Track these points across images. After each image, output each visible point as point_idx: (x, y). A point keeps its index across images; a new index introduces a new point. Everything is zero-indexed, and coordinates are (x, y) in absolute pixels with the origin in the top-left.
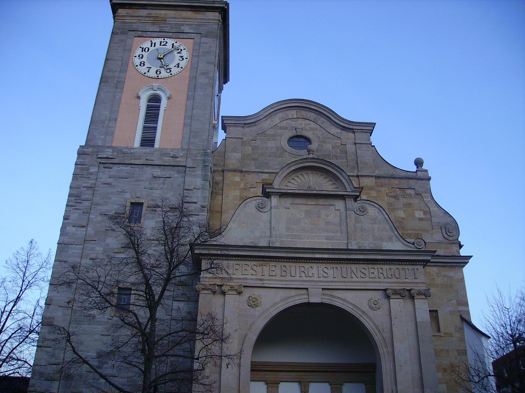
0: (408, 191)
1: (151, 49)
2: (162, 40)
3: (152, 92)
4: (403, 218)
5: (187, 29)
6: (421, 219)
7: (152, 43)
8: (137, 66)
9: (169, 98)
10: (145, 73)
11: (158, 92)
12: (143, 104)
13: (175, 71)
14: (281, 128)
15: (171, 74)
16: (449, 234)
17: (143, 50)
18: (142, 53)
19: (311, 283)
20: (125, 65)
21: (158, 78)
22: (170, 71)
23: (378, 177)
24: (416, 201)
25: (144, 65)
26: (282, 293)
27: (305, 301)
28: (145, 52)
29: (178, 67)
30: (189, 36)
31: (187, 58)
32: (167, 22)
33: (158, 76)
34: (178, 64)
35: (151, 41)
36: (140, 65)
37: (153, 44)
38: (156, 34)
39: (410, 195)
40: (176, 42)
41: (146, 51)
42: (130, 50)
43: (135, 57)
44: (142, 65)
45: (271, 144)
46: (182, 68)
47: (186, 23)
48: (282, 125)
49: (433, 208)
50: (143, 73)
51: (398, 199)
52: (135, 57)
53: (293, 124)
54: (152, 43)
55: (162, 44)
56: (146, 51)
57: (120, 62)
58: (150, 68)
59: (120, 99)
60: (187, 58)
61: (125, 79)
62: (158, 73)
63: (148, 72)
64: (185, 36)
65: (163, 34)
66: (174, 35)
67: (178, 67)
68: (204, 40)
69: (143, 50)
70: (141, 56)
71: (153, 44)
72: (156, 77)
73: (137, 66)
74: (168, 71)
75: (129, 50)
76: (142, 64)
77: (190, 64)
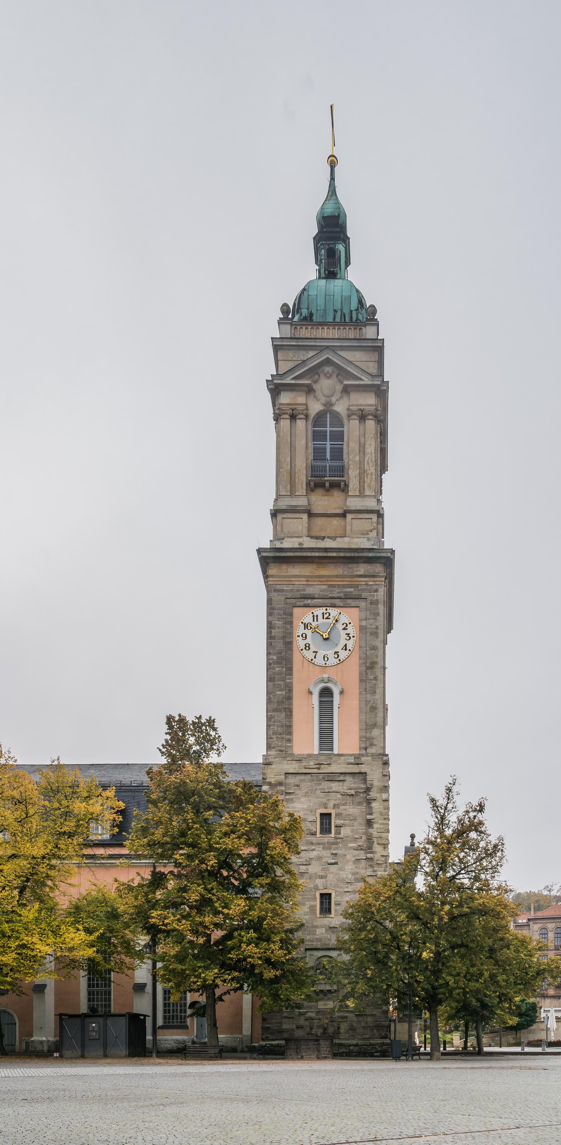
3: (323, 685)
7: (313, 616)
8: (302, 650)
9: (342, 693)
10: (312, 660)
11: (329, 685)
12: (315, 699)
13: (343, 655)
15: (340, 660)
17: (306, 626)
25: (309, 649)
29: (346, 649)
34: (346, 645)
35: (313, 613)
36: (305, 648)
41: (309, 628)
43: (298, 636)
44: (307, 648)
46: (350, 650)
50: (310, 660)
52: (298, 636)
55: (326, 616)
56: (309, 628)
58: (317, 652)
60: (353, 637)
63: (315, 657)
67: (346, 649)
70: (304, 635)
73: (302, 650)
74: (336, 656)
76: (307, 647)
77: (358, 640)
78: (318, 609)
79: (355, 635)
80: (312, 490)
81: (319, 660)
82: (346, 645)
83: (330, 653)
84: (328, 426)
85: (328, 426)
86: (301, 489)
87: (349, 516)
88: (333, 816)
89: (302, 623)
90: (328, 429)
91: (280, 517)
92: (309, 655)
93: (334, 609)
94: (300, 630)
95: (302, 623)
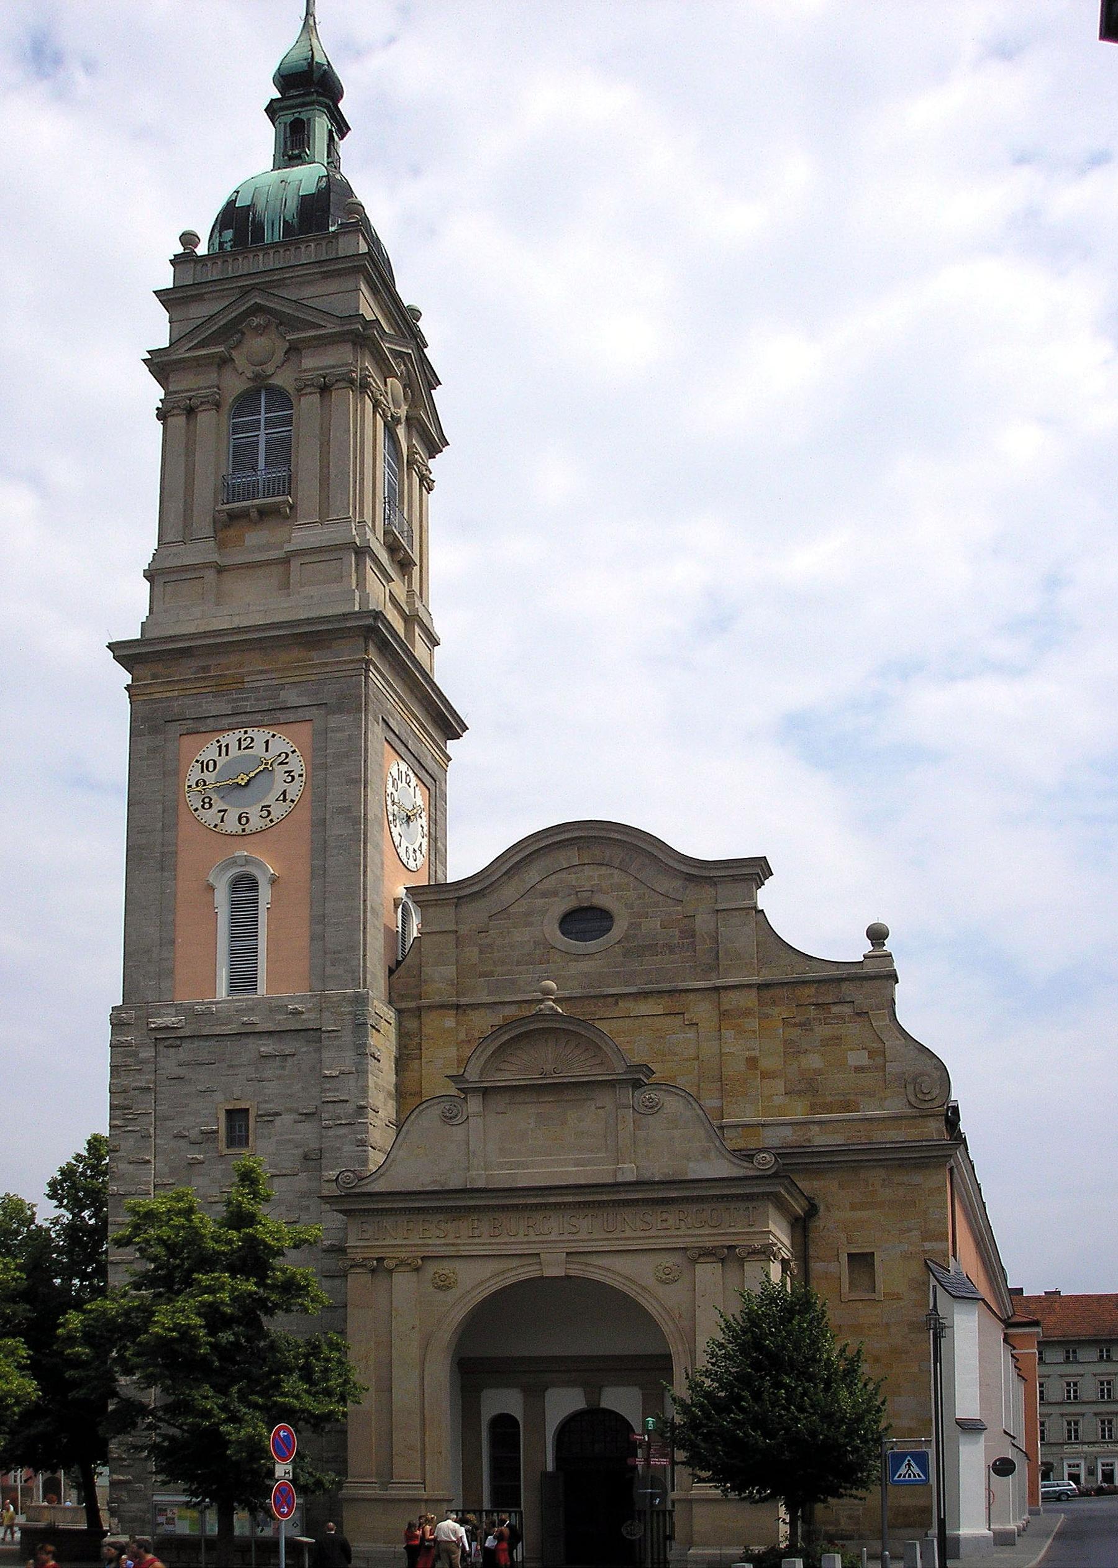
0: (835, 1009)
1: (222, 761)
2: (239, 734)
4: (819, 1072)
5: (291, 697)
6: (859, 1069)
7: (220, 747)
8: (196, 810)
10: (216, 826)
13: (279, 811)
14: (544, 895)
15: (271, 821)
16: (920, 1096)
17: (204, 766)
18: (203, 776)
19: (545, 1246)
20: (171, 811)
21: (244, 835)
22: (269, 813)
23: (761, 987)
24: (853, 1030)
25: (211, 805)
26: (492, 1267)
27: (537, 1274)
28: (210, 756)
30: (301, 714)
31: (301, 775)
32: (246, 685)
33: (244, 830)
34: (284, 793)
35: (218, 741)
36: (203, 807)
37: (224, 749)
38: (225, 722)
39: (841, 1018)
40: (274, 736)
41: (211, 769)
42: (176, 772)
44: (207, 806)
45: (522, 936)
46: (293, 801)
47: (291, 680)
48: (546, 885)
49: (892, 1043)
51: (812, 1030)
53: (571, 878)
54: (220, 747)
56: (211, 769)
57: (160, 806)
59: (174, 894)
60: (301, 775)
61: (176, 844)
62: (244, 821)
63: (222, 821)
64: (291, 716)
65: (240, 719)
66: (267, 719)
67: (284, 800)
68: (334, 721)
69: (204, 766)
71: (224, 749)
72: (240, 832)
73: (196, 810)
74: (265, 813)
75: (172, 773)
78: (231, 733)
79: (303, 772)
80: (227, 526)
81: (231, 825)
82: (284, 793)
83: (254, 812)
84: (263, 412)
85: (263, 412)
86: (203, 525)
87: (295, 564)
88: (252, 1114)
89: (197, 761)
90: (262, 416)
91: (160, 580)
92: (210, 816)
93: (262, 730)
94: (194, 774)
95: (197, 761)
